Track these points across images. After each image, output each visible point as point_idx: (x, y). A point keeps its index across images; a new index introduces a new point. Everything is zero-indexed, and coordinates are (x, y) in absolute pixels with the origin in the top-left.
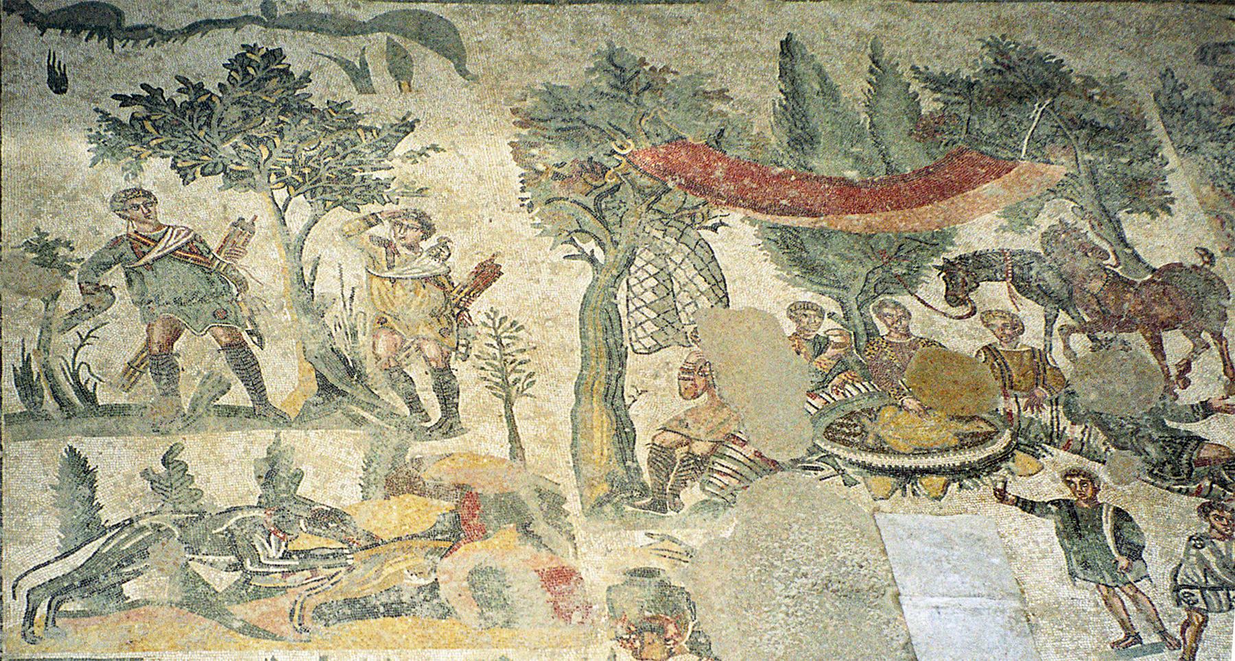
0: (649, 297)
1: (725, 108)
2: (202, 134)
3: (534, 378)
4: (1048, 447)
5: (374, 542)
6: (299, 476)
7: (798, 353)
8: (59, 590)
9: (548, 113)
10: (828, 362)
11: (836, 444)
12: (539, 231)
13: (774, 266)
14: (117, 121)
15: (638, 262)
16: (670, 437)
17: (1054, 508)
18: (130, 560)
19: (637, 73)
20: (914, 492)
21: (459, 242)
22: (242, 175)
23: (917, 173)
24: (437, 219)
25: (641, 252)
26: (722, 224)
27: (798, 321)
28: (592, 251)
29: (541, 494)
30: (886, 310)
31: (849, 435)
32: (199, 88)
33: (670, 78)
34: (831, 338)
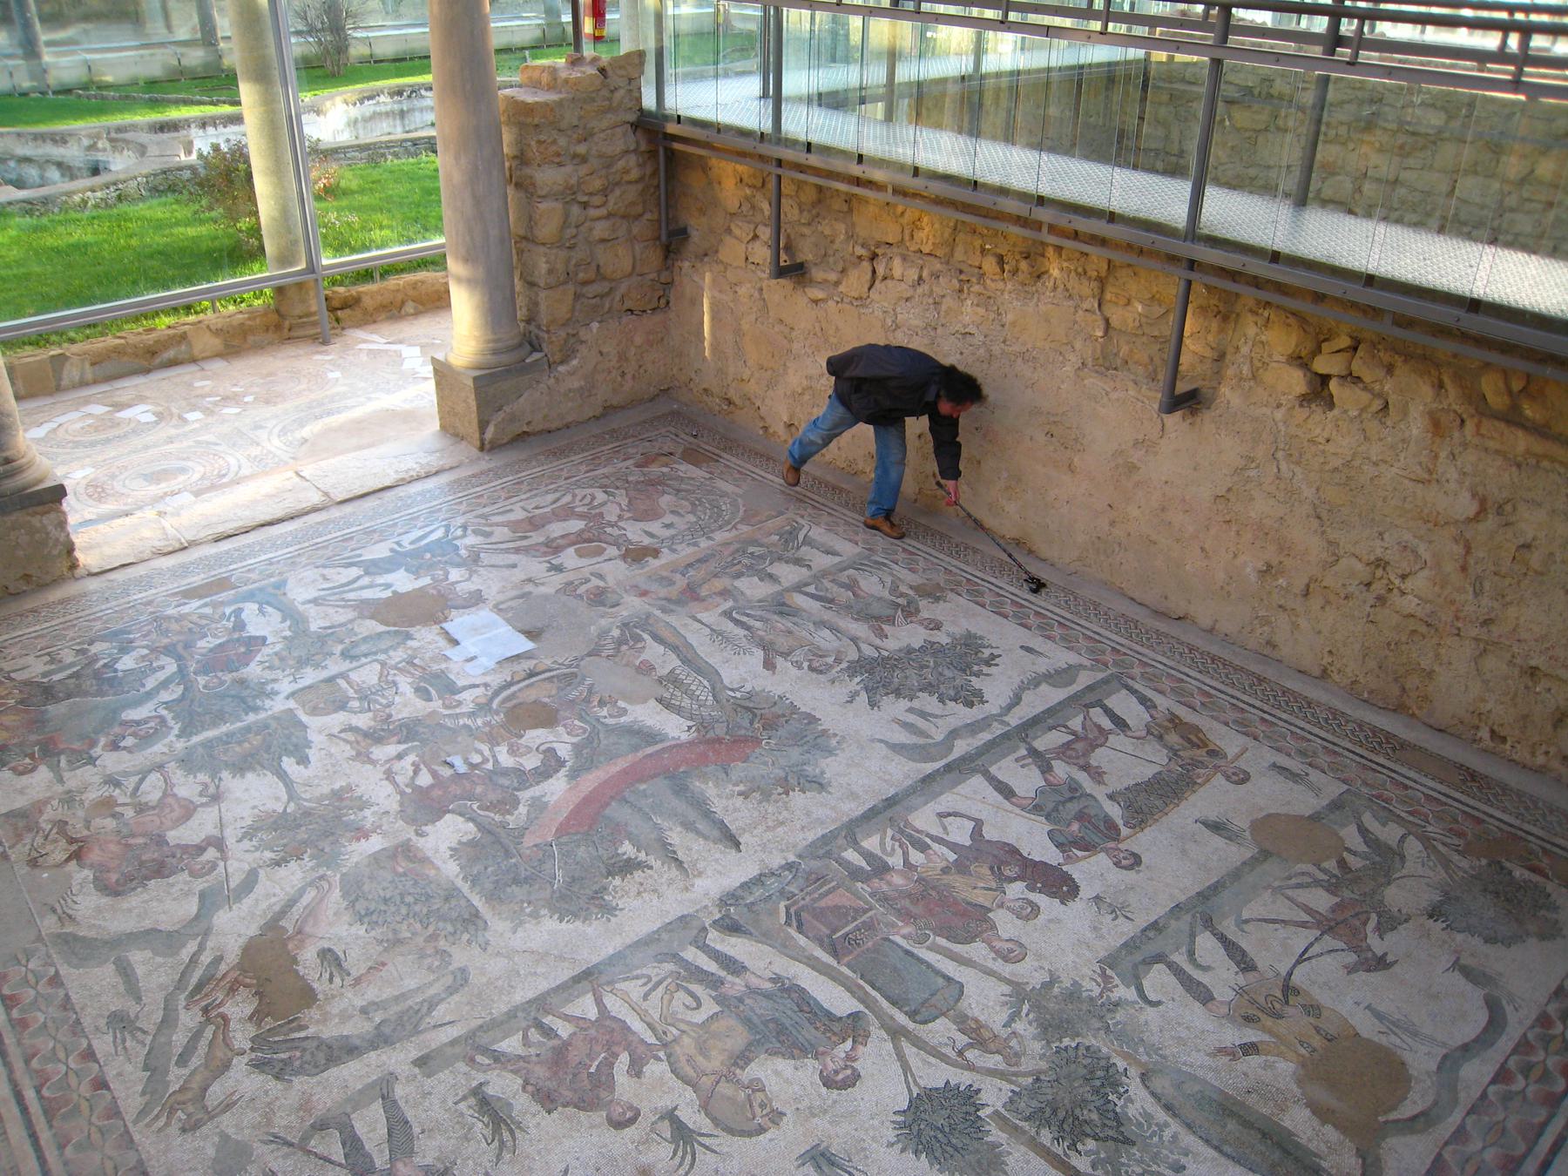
1: (737, 789)
9: (819, 740)
15: (710, 698)
21: (794, 671)
23: (608, 804)
24: (814, 675)
29: (672, 611)
33: (780, 790)
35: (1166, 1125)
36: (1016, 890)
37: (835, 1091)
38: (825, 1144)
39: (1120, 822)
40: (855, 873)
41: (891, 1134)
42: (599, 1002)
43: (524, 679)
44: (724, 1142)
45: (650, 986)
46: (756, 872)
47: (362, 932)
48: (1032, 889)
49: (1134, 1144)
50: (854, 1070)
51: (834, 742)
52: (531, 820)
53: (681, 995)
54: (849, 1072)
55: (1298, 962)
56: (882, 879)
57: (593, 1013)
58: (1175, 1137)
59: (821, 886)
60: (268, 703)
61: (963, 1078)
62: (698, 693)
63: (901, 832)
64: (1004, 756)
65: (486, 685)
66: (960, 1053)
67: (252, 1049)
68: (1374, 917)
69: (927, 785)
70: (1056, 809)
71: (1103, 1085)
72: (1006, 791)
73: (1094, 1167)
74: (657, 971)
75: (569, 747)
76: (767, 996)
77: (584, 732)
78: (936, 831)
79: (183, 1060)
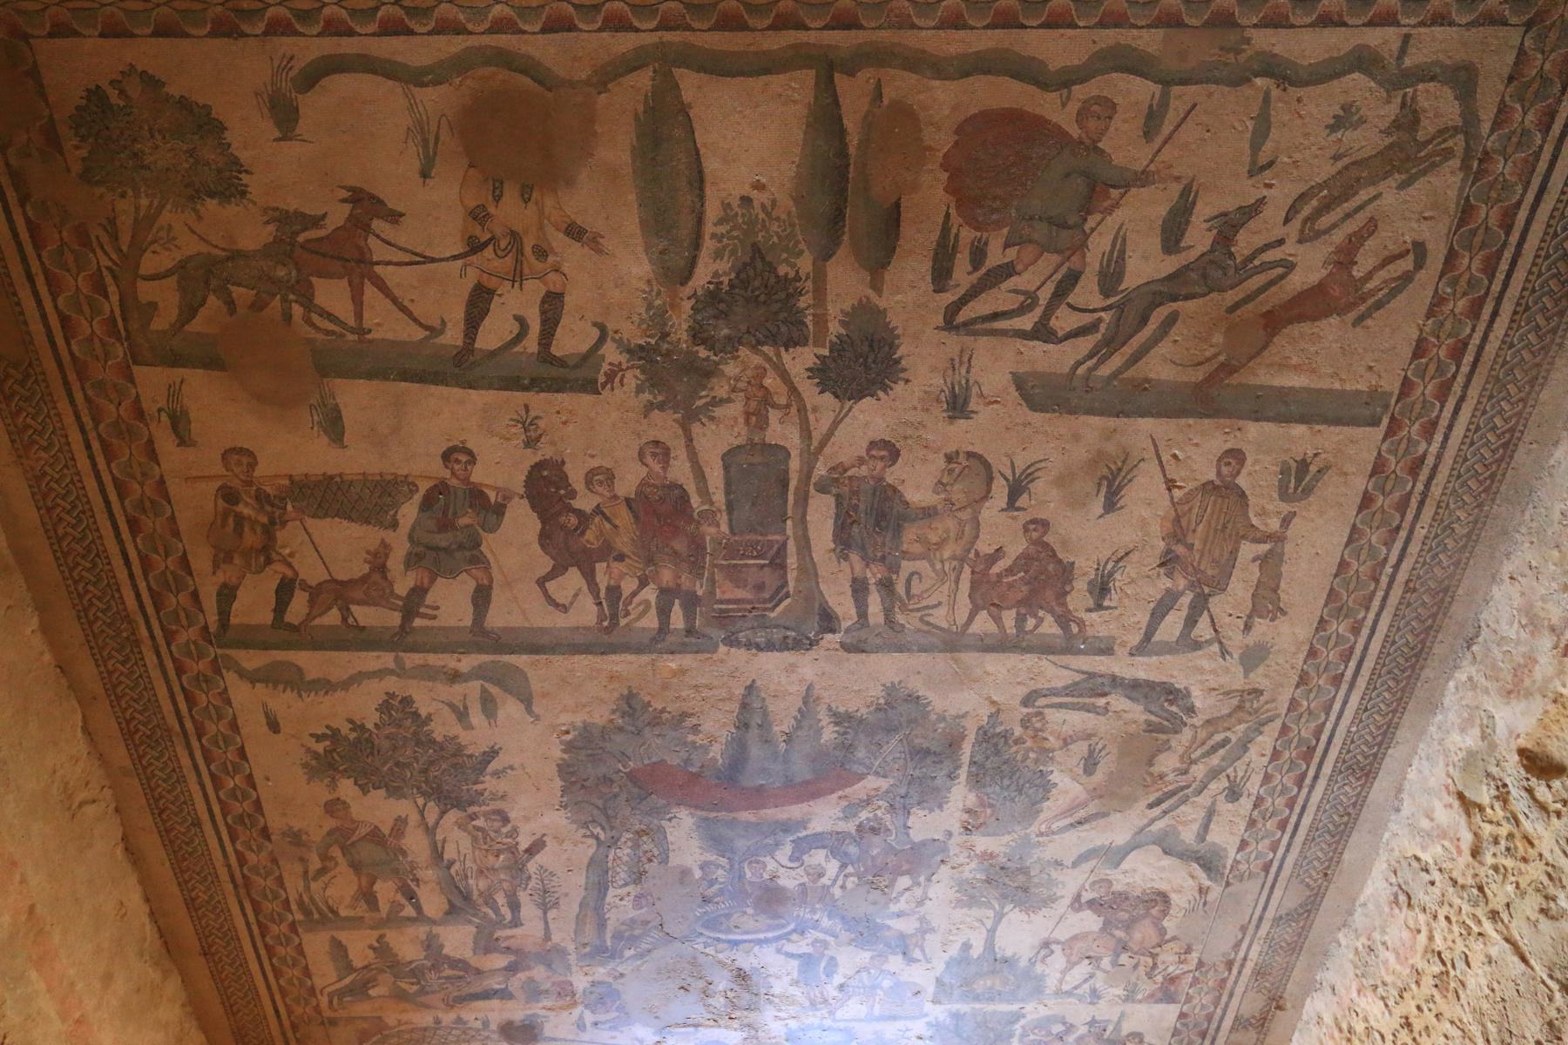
2: (369, 760)
5: (478, 972)
6: (442, 946)
8: (341, 993)
14: (316, 753)
18: (369, 982)
22: (398, 789)
24: (512, 815)
32: (362, 727)
35: (713, 236)
36: (585, 502)
37: (897, 445)
38: (945, 415)
39: (418, 498)
40: (691, 602)
41: (899, 388)
43: (745, 941)
44: (1000, 464)
47: (1056, 774)
48: (573, 494)
49: (754, 245)
50: (869, 450)
53: (914, 591)
54: (874, 452)
55: (433, 260)
56: (679, 585)
58: (721, 222)
59: (728, 610)
60: (941, 1017)
61: (808, 389)
63: (614, 617)
64: (444, 629)
65: (779, 951)
66: (788, 406)
67: (1186, 725)
68: (301, 238)
69: (537, 644)
70: (461, 547)
71: (721, 301)
72: (482, 598)
73: (801, 253)
76: (863, 548)
77: (750, 863)
78: (588, 602)
79: (1226, 741)
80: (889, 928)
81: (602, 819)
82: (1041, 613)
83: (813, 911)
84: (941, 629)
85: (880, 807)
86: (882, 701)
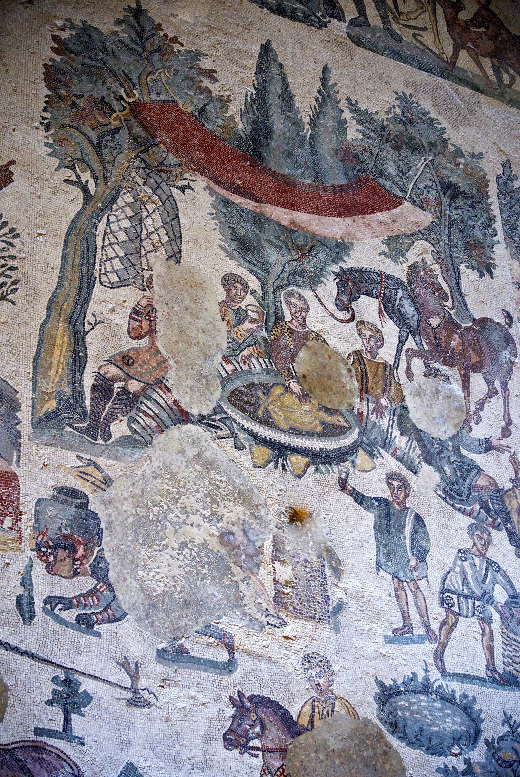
0: (122, 236)
3: (18, 286)
4: (382, 451)
7: (223, 320)
9: (78, 48)
10: (243, 333)
11: (235, 409)
12: (50, 151)
13: (220, 237)
15: (120, 202)
16: (113, 370)
17: (376, 504)
19: (154, 35)
20: (283, 466)
25: (124, 194)
26: (190, 187)
27: (228, 291)
28: (87, 182)
30: (293, 300)
31: (245, 403)
33: (176, 47)
34: (250, 313)
42: (456, 54)
45: (417, 32)
46: (274, 16)
51: (65, 35)
52: (413, 236)
53: (401, 8)
57: (463, 54)
62: (126, 224)
74: (407, 35)
75: (320, 290)
77: (290, 295)
80: (480, 471)
81: (92, 158)
82: (511, 71)
83: (379, 411)
84: (434, 53)
85: (426, 251)
86: (398, 111)
